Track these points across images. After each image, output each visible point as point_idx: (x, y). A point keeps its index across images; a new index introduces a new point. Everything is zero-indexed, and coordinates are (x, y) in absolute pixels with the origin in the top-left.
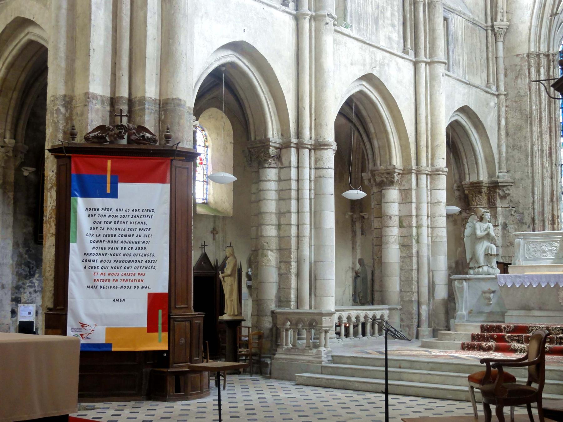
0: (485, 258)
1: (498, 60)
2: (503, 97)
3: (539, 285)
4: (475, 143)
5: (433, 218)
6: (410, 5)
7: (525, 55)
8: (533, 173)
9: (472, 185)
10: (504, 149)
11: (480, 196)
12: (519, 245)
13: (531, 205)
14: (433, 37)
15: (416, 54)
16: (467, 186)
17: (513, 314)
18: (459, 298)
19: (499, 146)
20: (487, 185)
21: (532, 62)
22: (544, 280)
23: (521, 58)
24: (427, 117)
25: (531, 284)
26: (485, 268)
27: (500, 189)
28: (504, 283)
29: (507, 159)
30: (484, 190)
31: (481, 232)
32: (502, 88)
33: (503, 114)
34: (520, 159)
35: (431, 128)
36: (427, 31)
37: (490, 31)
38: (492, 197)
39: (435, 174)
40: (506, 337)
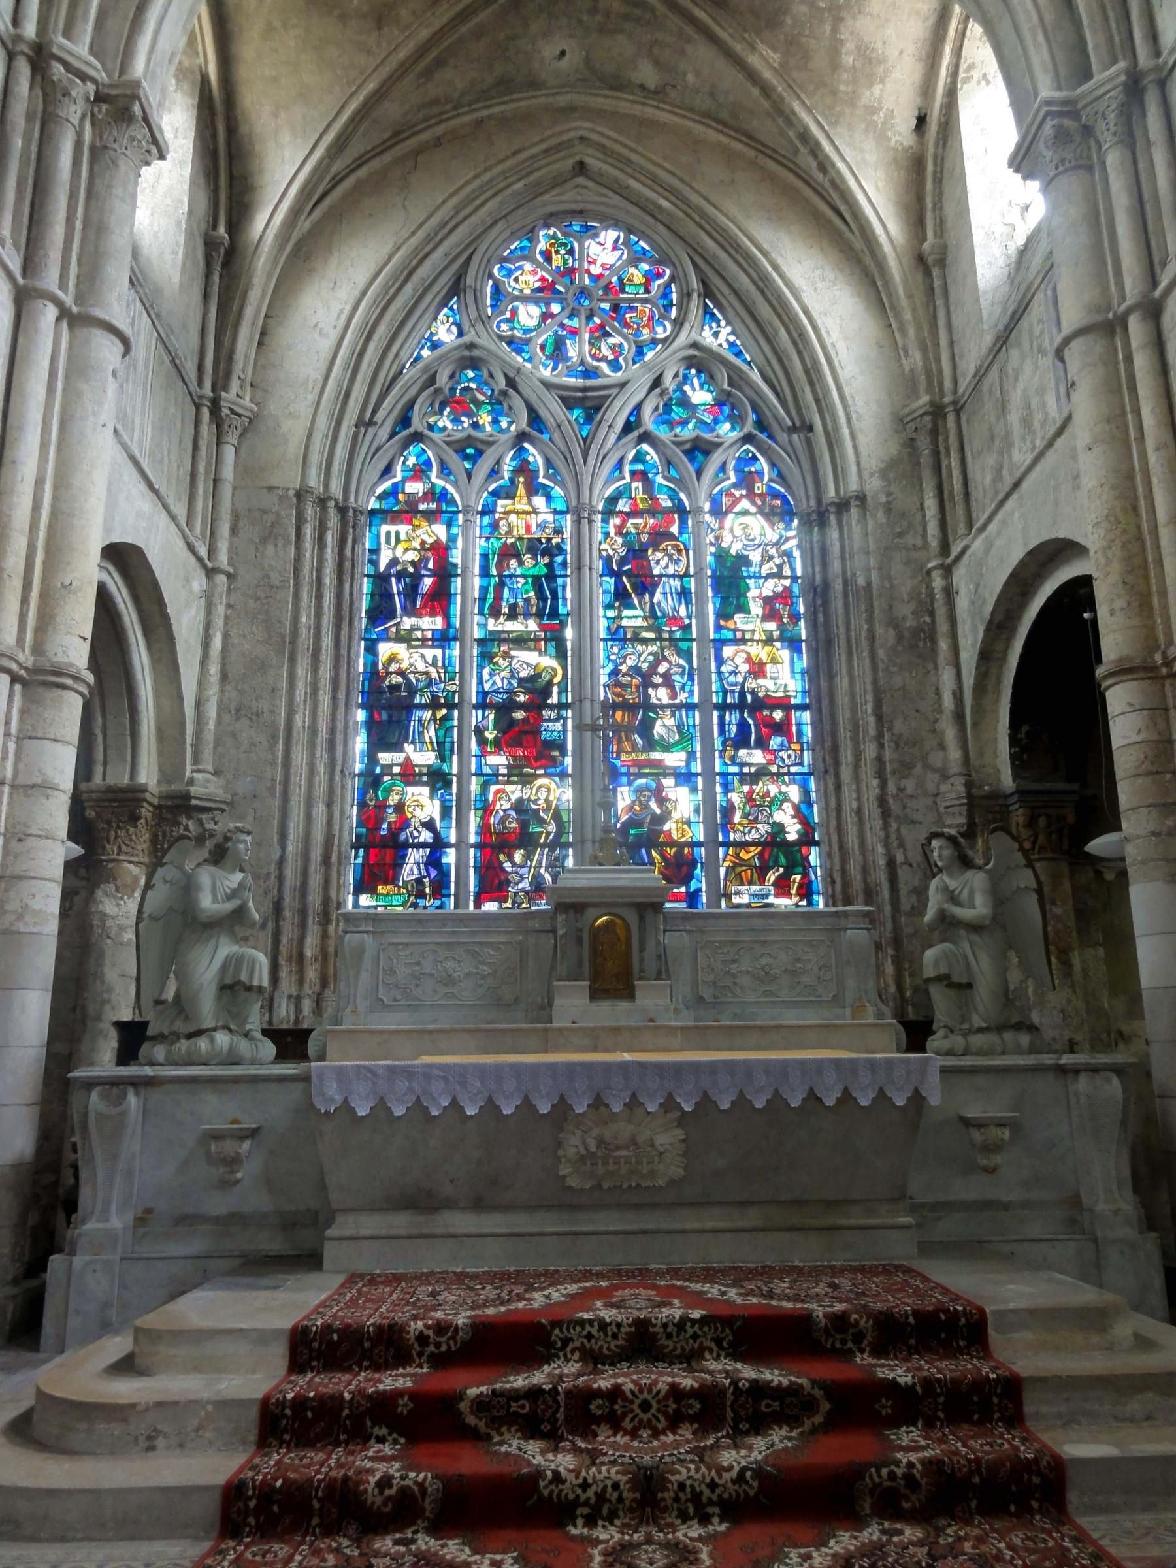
0: (219, 998)
1: (220, 486)
2: (223, 578)
3: (527, 1105)
4: (139, 676)
5: (14, 844)
6: (30, 117)
7: (291, 493)
8: (286, 782)
9: (111, 796)
10: (212, 711)
11: (132, 830)
12: (359, 953)
13: (273, 868)
14: (96, 247)
15: (29, 265)
16: (94, 796)
17: (364, 1232)
18: (99, 1159)
19: (199, 703)
20: (156, 802)
21: (310, 511)
22: (510, 1085)
23: (281, 497)
24: (39, 482)
25: (454, 1103)
26: (222, 1039)
27: (189, 817)
28: (339, 1098)
29: (218, 742)
30: (146, 812)
31: (215, 900)
32: (223, 558)
33: (219, 622)
34: (253, 744)
35: (50, 526)
36: (79, 225)
37: (206, 412)
38: (164, 835)
39: (45, 684)
40: (463, 1406)
